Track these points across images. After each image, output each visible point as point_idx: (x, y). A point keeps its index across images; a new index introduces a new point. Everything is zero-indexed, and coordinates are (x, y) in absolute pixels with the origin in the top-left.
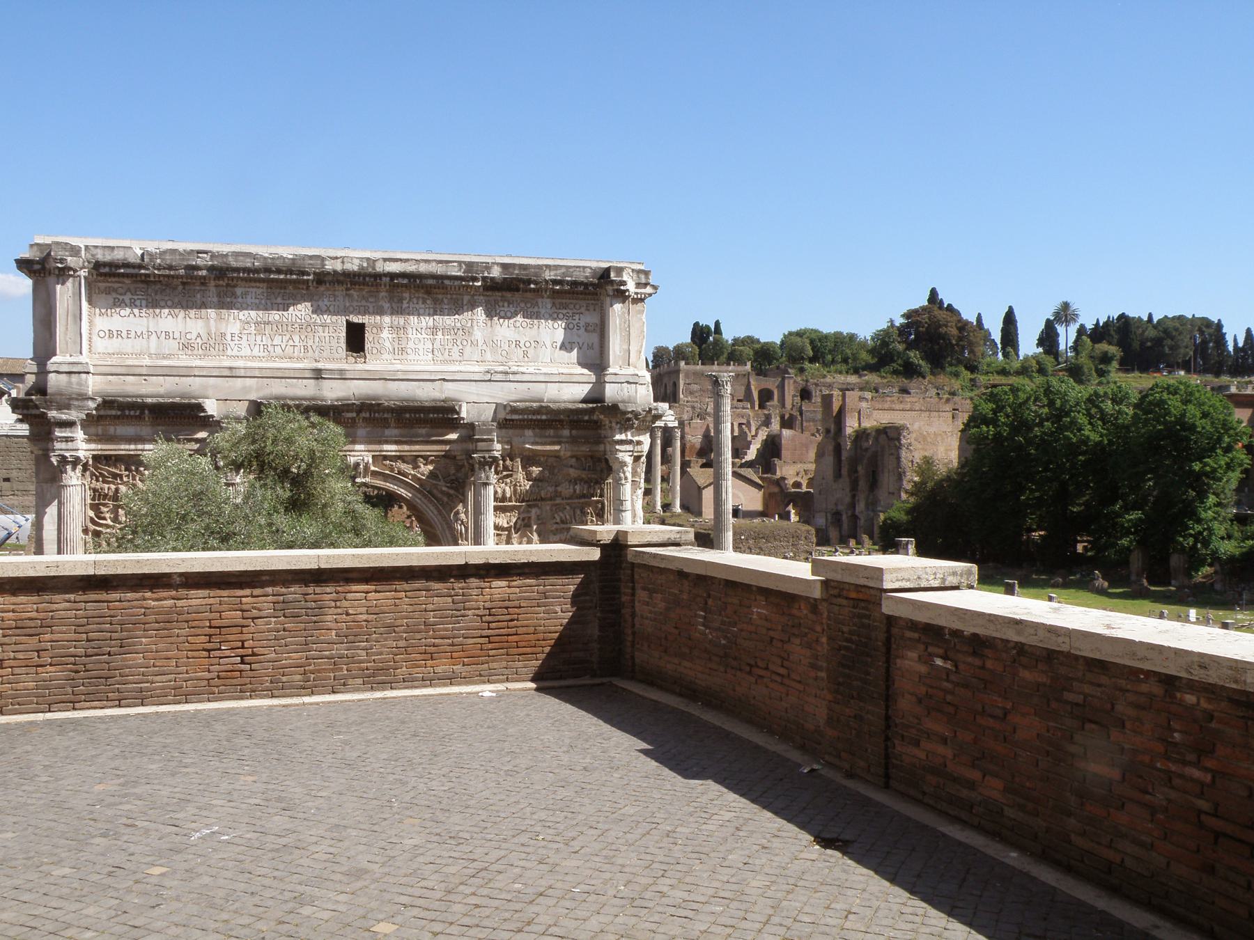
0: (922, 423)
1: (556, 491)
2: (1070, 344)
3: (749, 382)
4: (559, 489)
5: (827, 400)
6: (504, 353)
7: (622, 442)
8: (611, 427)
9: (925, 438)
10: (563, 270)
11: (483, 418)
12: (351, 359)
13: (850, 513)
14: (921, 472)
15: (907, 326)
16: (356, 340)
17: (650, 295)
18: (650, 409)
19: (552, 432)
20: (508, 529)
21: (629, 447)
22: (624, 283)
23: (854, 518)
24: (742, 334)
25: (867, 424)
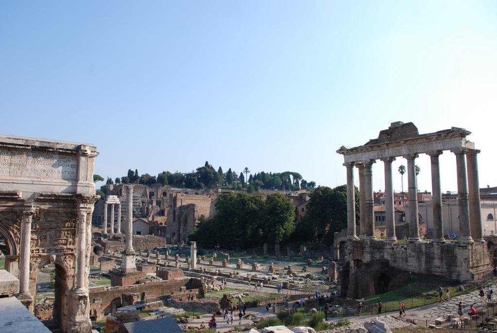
1: (57, 226)
2: (248, 180)
3: (146, 190)
4: (58, 225)
5: (171, 195)
6: (39, 174)
7: (83, 208)
9: (203, 209)
10: (64, 145)
13: (178, 233)
17: (96, 156)
19: (56, 204)
21: (86, 210)
22: (86, 151)
23: (179, 235)
24: (144, 173)
25: (184, 204)
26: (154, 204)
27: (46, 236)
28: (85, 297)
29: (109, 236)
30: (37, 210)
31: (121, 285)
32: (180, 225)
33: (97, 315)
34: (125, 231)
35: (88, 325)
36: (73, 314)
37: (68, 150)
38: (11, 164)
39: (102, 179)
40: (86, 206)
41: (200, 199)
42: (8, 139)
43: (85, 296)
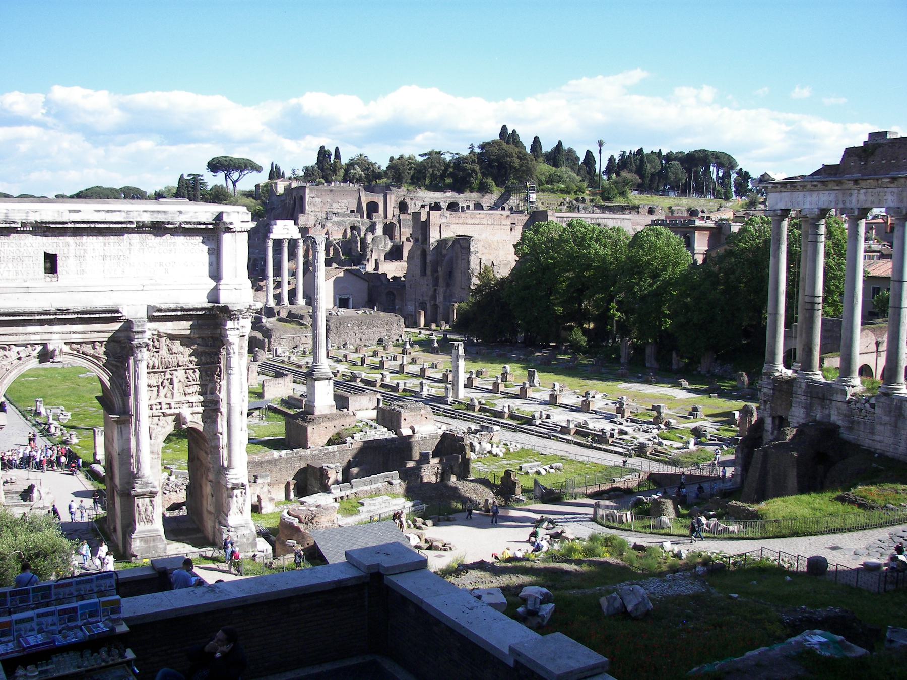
0: (488, 234)
2: (603, 169)
5: (416, 215)
8: (225, 320)
10: (192, 214)
11: (139, 316)
12: (49, 279)
13: (432, 303)
14: (480, 276)
15: (481, 154)
16: (51, 263)
18: (250, 306)
20: (158, 386)
21: (237, 332)
22: (231, 223)
23: (436, 307)
26: (379, 231)
27: (171, 379)
28: (243, 485)
29: (278, 313)
30: (153, 335)
31: (305, 447)
32: (436, 283)
33: (263, 504)
34: (311, 299)
35: (249, 532)
36: (223, 512)
37: (200, 223)
38: (104, 257)
39: (258, 169)
40: (237, 326)
41: (484, 221)
42: (96, 213)
43: (242, 483)
